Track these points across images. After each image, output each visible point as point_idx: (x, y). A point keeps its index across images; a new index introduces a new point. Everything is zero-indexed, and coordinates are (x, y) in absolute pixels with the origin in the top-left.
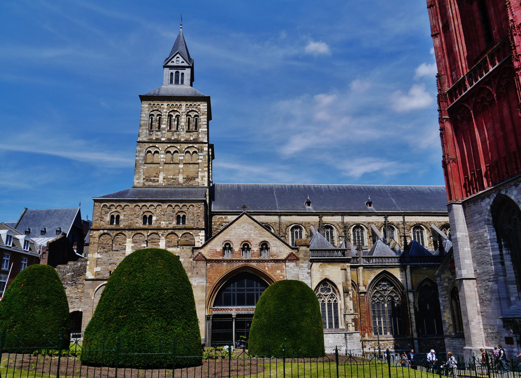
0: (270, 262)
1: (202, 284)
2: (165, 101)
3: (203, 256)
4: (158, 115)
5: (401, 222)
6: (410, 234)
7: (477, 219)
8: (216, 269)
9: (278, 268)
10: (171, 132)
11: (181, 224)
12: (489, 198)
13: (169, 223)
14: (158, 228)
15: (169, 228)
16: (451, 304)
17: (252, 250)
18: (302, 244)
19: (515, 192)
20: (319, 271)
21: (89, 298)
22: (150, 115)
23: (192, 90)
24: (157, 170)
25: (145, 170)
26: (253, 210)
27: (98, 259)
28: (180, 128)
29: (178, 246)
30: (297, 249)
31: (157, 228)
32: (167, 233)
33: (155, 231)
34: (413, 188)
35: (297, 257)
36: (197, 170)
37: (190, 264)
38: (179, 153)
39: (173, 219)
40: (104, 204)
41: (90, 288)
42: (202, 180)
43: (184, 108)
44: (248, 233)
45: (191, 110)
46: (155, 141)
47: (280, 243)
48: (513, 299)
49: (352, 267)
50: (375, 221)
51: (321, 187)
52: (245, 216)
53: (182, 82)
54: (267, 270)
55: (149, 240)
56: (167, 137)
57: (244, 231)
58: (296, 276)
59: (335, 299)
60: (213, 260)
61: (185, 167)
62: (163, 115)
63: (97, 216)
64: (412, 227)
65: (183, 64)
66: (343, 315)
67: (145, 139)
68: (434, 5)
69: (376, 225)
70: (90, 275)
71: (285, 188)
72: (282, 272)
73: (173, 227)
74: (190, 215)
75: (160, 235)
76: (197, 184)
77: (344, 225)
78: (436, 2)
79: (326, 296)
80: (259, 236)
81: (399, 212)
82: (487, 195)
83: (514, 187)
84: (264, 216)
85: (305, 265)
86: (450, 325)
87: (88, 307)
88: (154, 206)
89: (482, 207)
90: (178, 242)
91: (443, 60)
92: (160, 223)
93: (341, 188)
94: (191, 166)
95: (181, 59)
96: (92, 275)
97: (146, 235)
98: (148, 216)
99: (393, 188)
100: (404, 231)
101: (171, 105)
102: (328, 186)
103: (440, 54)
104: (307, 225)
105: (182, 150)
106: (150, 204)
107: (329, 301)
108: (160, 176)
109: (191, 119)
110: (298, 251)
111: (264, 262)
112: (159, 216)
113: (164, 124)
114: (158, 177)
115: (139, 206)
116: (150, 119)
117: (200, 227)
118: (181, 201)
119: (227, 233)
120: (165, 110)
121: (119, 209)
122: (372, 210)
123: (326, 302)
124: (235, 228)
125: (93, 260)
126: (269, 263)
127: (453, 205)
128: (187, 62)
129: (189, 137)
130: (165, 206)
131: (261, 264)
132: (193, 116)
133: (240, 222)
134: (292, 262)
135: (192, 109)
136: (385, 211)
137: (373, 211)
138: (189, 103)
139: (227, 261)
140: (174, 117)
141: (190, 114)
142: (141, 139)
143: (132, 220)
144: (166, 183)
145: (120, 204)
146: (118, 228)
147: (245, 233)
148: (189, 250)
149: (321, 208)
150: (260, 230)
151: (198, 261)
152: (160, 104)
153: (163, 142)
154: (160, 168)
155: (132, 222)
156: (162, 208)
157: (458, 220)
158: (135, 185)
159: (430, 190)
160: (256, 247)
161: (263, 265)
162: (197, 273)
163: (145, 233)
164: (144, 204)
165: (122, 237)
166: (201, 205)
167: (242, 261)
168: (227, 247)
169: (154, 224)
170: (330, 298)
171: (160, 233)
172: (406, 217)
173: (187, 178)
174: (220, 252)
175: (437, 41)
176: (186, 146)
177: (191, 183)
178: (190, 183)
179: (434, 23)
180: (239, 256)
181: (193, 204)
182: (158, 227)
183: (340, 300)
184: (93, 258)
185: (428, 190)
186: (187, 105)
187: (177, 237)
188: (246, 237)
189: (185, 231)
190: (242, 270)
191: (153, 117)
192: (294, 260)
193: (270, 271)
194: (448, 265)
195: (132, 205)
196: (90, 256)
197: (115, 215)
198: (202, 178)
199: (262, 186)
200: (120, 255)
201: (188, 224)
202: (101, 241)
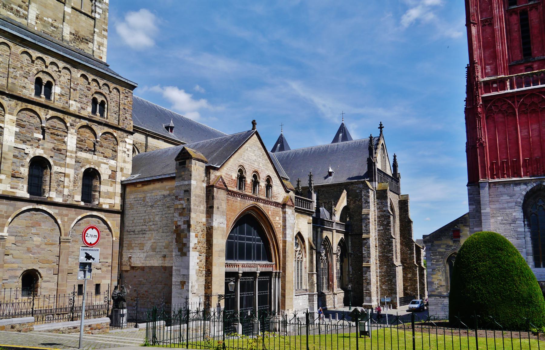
3: (224, 183)
11: (98, 114)
12: (526, 185)
13: (82, 108)
14: (65, 110)
29: (94, 151)
31: (62, 109)
32: (79, 125)
42: (99, 49)
55: (48, 129)
57: (255, 158)
66: (307, 275)
75: (68, 125)
76: (91, 53)
82: (525, 183)
86: (441, 286)
88: (58, 68)
89: (514, 190)
90: (95, 145)
97: (44, 117)
117: (127, 129)
130: (77, 74)
133: (251, 142)
155: (15, 81)
163: (43, 113)
171: (69, 120)
173: (76, 35)
174: (235, 180)
177: (82, 46)
183: (306, 257)
187: (93, 135)
189: (106, 129)
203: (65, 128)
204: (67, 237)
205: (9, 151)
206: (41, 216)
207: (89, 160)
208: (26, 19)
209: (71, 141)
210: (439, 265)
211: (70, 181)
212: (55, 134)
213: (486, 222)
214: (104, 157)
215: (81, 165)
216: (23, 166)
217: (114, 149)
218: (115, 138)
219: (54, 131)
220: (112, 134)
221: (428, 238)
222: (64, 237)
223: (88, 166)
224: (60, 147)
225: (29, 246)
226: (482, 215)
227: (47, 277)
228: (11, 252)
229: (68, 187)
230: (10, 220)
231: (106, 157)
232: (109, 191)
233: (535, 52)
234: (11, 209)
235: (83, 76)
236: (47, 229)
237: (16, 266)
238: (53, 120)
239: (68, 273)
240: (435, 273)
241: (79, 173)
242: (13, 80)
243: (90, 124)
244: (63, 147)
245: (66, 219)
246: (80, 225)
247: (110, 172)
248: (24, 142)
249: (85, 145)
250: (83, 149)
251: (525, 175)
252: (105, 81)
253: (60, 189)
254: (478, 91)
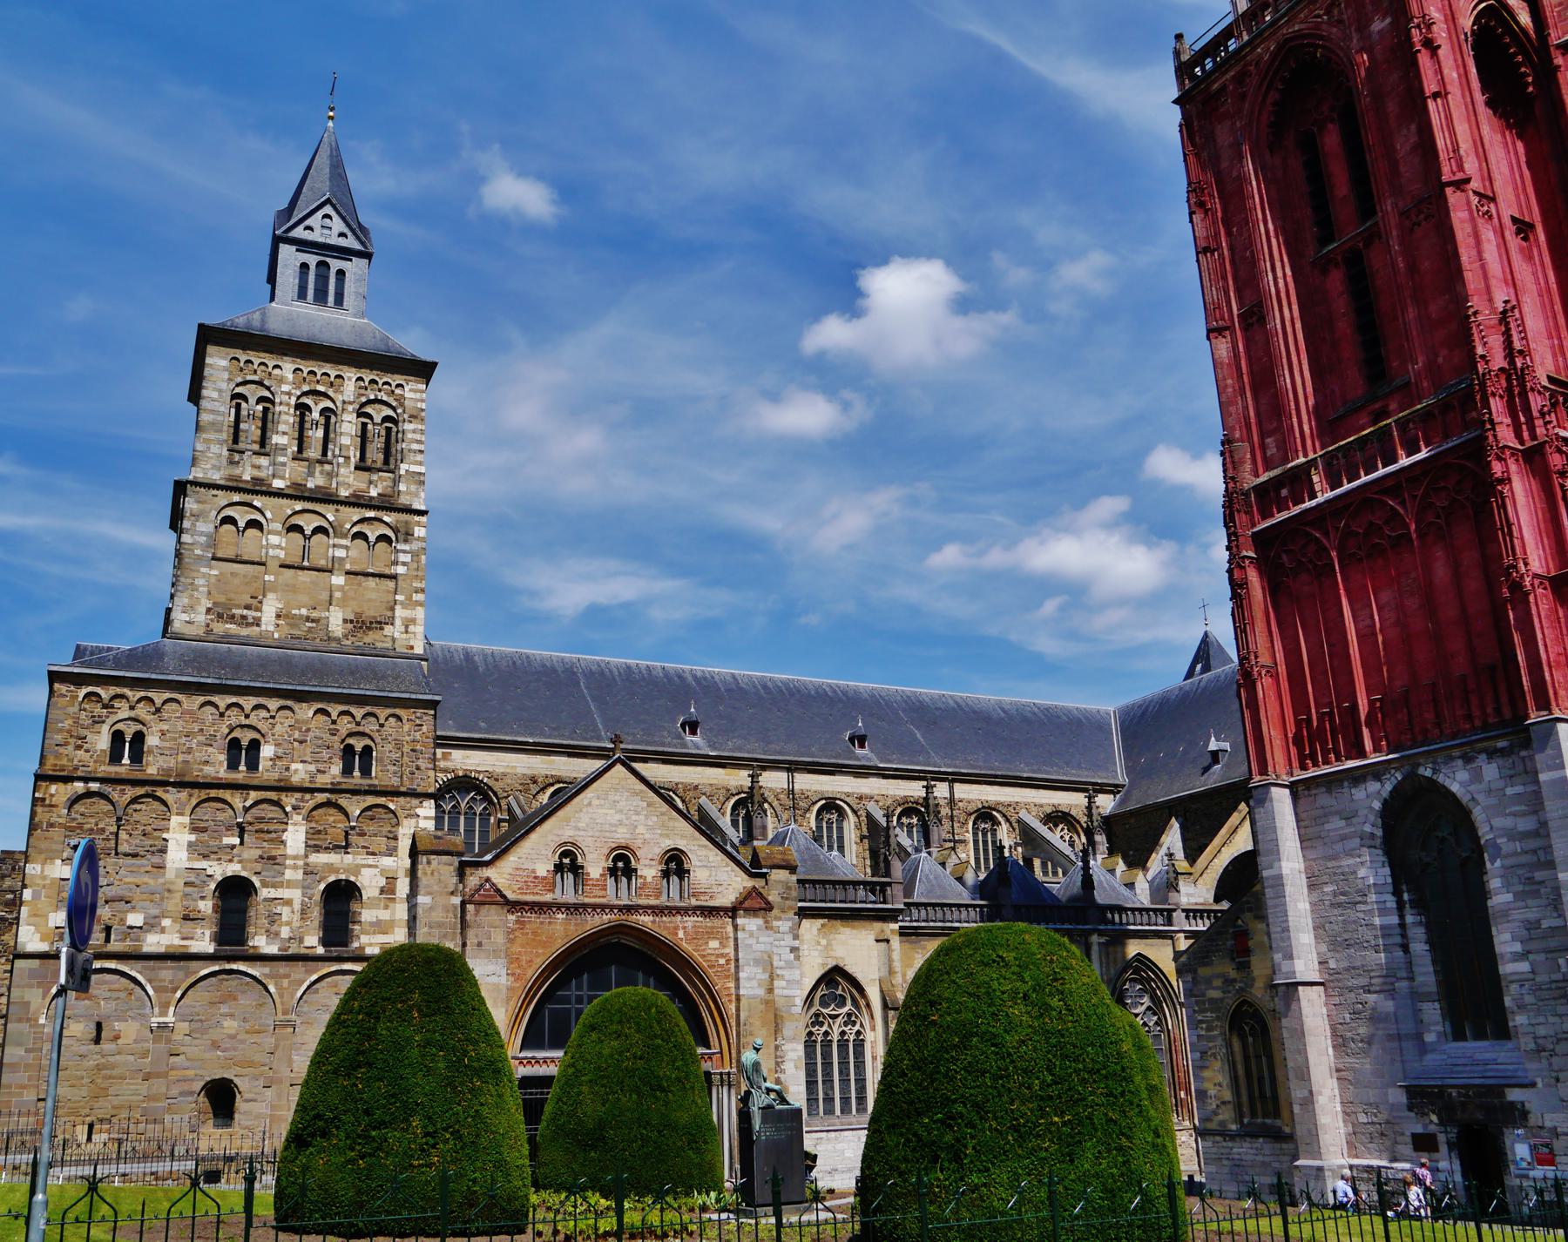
0: (690, 913)
1: (494, 979)
2: (286, 355)
3: (498, 891)
4: (261, 400)
5: (945, 798)
6: (966, 834)
7: (1336, 830)
8: (535, 933)
9: (711, 934)
10: (306, 463)
11: (357, 773)
12: (1379, 780)
13: (318, 771)
15: (318, 786)
16: (1229, 1045)
17: (641, 876)
18: (775, 861)
19: (1463, 775)
20: (819, 943)
21: (29, 1020)
22: (235, 396)
23: (374, 333)
24: (255, 585)
25: (213, 580)
26: (531, 735)
27: (63, 883)
28: (337, 452)
29: (346, 847)
30: (764, 876)
31: (276, 784)
32: (311, 804)
33: (272, 795)
34: (960, 701)
35: (768, 903)
36: (391, 598)
37: (451, 915)
38: (332, 534)
39: (331, 758)
40: (90, 689)
41: (31, 986)
42: (407, 632)
43: (349, 389)
44: (627, 822)
45: (372, 397)
46: (249, 487)
47: (719, 858)
48: (1430, 1038)
49: (904, 933)
50: (876, 792)
51: (713, 677)
52: (619, 767)
53: (339, 301)
54: (681, 939)
55: (250, 824)
56: (290, 478)
57: (618, 817)
58: (766, 958)
59: (857, 1027)
60: (526, 903)
61: (352, 584)
62: (277, 400)
63: (60, 731)
64: (971, 814)
65: (342, 242)
67: (216, 477)
68: (1215, 250)
69: (881, 804)
70: (31, 940)
71: (610, 671)
72: (724, 947)
73: (332, 783)
74: (388, 747)
75: (288, 809)
76: (389, 645)
77: (793, 798)
78: (1224, 244)
79: (835, 1017)
80: (659, 832)
81: (942, 770)
82: (1376, 772)
83: (1460, 762)
84: (564, 759)
85: (784, 925)
86: (1224, 1103)
87: (23, 1053)
88: (269, 711)
89: (1353, 800)
90: (347, 834)
91: (1240, 402)
92: (288, 769)
93: (770, 684)
94: (372, 582)
95: (338, 225)
96: (42, 940)
97: (241, 805)
98: (245, 743)
99: (908, 697)
100: (953, 827)
101: (306, 371)
102: (732, 674)
103: (1229, 381)
104: (691, 794)
105: (342, 526)
106: (254, 701)
107: (843, 1033)
108: (265, 608)
109: (370, 427)
110: (767, 884)
111: (674, 912)
112: (286, 745)
113: (284, 433)
115: (217, 707)
116: (233, 410)
117: (420, 790)
118: (360, 700)
119: (568, 820)
121: (142, 711)
122: (869, 759)
123: (835, 1037)
124: (590, 804)
125: (44, 886)
126: (687, 918)
127: (1274, 790)
128: (358, 238)
129: (363, 486)
130: (306, 711)
131: (664, 918)
132: (378, 419)
134: (756, 916)
135: (376, 396)
136: (904, 763)
137: (871, 764)
138: (368, 376)
139: (576, 909)
140: (316, 415)
141: (368, 410)
142: (200, 475)
143: (189, 751)
144: (286, 630)
145: (150, 694)
146: (138, 776)
147: (620, 823)
148: (447, 867)
149: (730, 743)
150: (663, 814)
151: (482, 907)
152: (271, 364)
153: (279, 494)
154: (267, 578)
155: (189, 758)
156: (297, 717)
157: (1282, 828)
158: (177, 631)
159: (1003, 710)
160: (651, 866)
161: (670, 922)
162: (480, 944)
163: (237, 800)
164: (234, 700)
165: (155, 811)
166: (425, 718)
167: (611, 910)
168: (569, 863)
169: (267, 771)
170: (846, 1024)
171: (289, 801)
172: (957, 786)
173: (358, 622)
174: (544, 878)
175: (1223, 347)
176: (356, 514)
177: (370, 637)
178: (367, 640)
179: (1215, 297)
180: (601, 893)
181: (398, 711)
182: (280, 780)
183: (873, 1029)
184: (44, 878)
185: (1000, 711)
186: (360, 379)
187: (342, 817)
188: (622, 836)
189: (371, 800)
190: (607, 936)
191: (244, 405)
192: (760, 909)
193: (691, 940)
194: (1224, 944)
195: (192, 702)
196: (33, 872)
197: (129, 730)
198: (407, 627)
199: (538, 659)
200: (143, 870)
201: (381, 774)
202: (74, 819)
203: (283, 816)
204: (288, 1017)
205: (177, 877)
206: (236, 982)
207: (335, 866)
208: (258, 625)
209: (295, 837)
210: (1212, 1039)
211: (293, 912)
212: (263, 832)
213: (1276, 906)
214: (368, 853)
215: (318, 877)
216: (202, 898)
217: (391, 836)
218: (393, 812)
219: (262, 826)
220: (387, 808)
221: (1183, 959)
222: (282, 1018)
223: (332, 878)
224: (274, 853)
225: (215, 1038)
226: (1266, 884)
227: (251, 1092)
228: (182, 1049)
229: (288, 923)
230: (178, 994)
231: (373, 854)
232: (381, 918)
233: (1395, 364)
234: (181, 974)
235: (319, 711)
236: (250, 1005)
237: (191, 1073)
238: (259, 807)
239: (291, 1085)
240: (1208, 1063)
241: (313, 895)
242: (186, 755)
243: (333, 797)
244: (280, 852)
245: (285, 982)
246: (317, 991)
247: (383, 882)
248: (205, 857)
249: (326, 839)
250: (321, 847)
251: (1377, 749)
252: (368, 708)
253: (274, 928)
254: (1235, 523)
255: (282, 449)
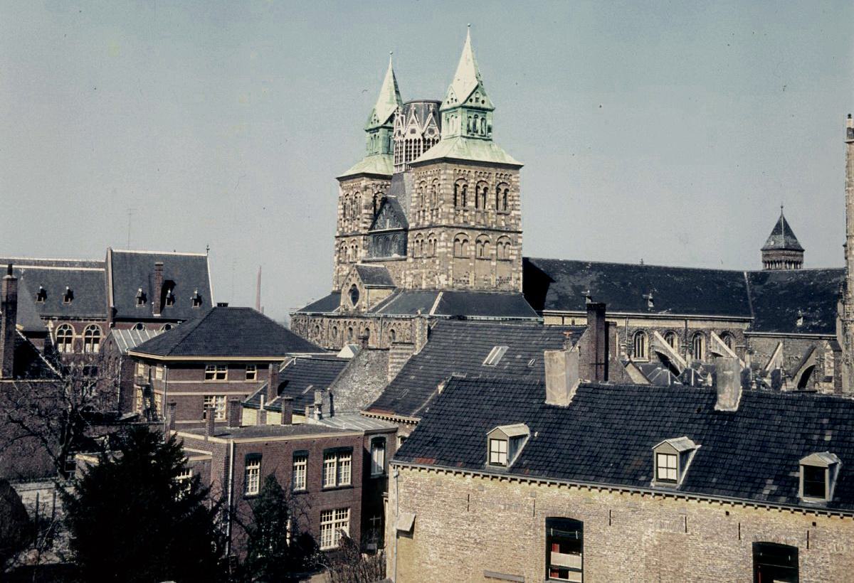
28: (490, 207)
114: (468, 277)
120: (472, 181)
255: (471, 209)
